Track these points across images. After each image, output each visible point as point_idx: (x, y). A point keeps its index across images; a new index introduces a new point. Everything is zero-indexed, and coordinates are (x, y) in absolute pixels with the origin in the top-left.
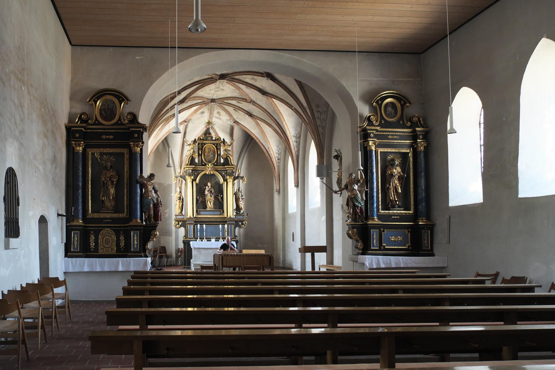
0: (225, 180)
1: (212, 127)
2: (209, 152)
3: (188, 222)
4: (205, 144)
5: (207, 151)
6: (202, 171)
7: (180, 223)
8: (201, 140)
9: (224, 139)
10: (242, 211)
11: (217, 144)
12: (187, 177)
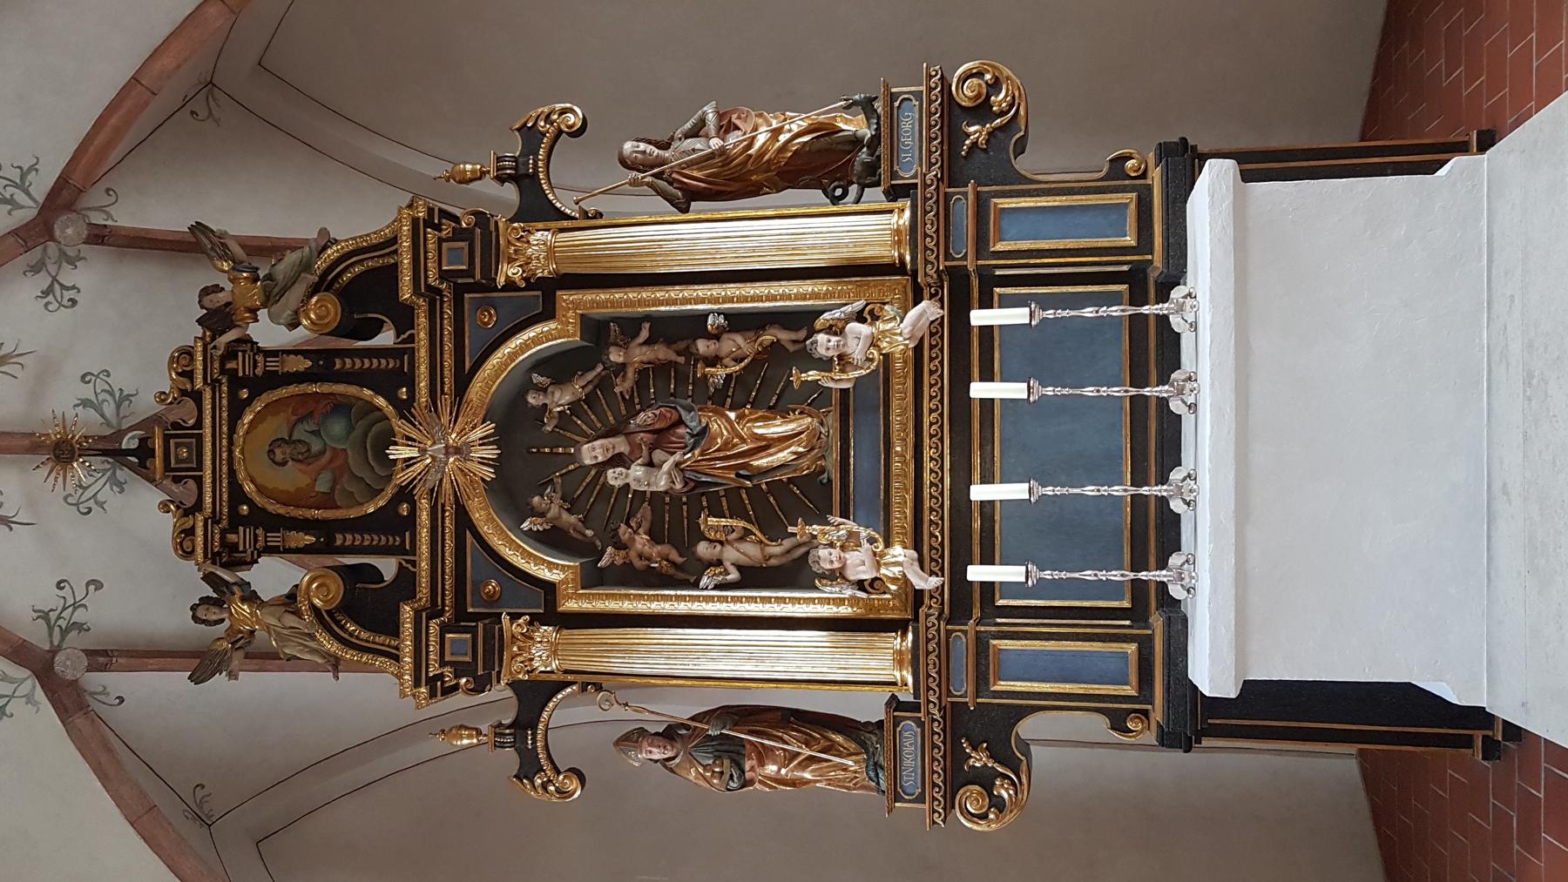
0: (543, 295)
2: (307, 458)
3: (964, 691)
4: (237, 494)
5: (291, 478)
6: (464, 521)
7: (979, 760)
8: (190, 532)
10: (854, 125)
11: (236, 382)
12: (515, 669)
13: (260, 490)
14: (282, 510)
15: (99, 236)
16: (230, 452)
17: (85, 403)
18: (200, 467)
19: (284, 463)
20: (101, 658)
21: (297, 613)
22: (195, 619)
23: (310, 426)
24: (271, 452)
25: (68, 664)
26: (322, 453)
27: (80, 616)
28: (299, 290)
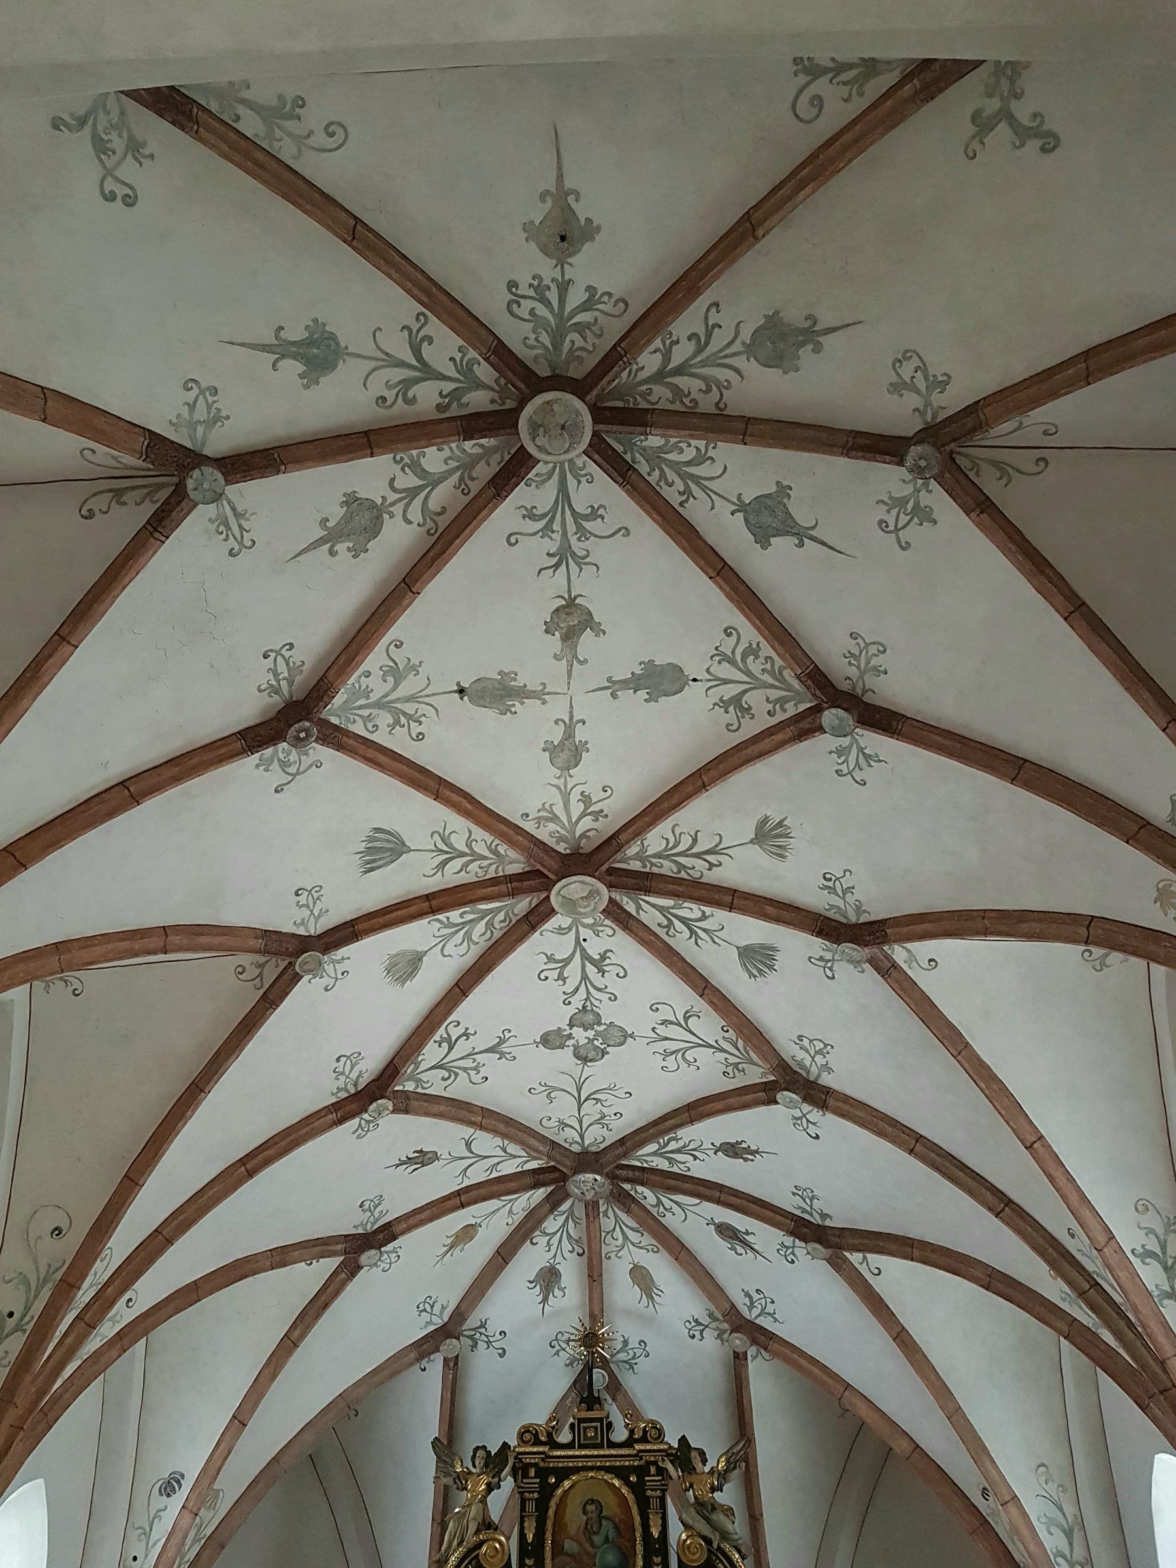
1: (615, 1387)
2: (589, 1531)
4: (563, 1474)
5: (575, 1518)
8: (538, 1442)
9: (683, 1440)
11: (642, 1471)
13: (566, 1492)
14: (551, 1513)
15: (739, 1359)
16: (592, 1469)
17: (626, 1343)
18: (581, 1447)
19: (585, 1512)
20: (453, 1365)
21: (477, 1532)
22: (477, 1448)
23: (612, 1534)
24: (592, 1501)
25: (450, 1347)
26: (593, 1545)
27: (482, 1345)
28: (707, 1531)
